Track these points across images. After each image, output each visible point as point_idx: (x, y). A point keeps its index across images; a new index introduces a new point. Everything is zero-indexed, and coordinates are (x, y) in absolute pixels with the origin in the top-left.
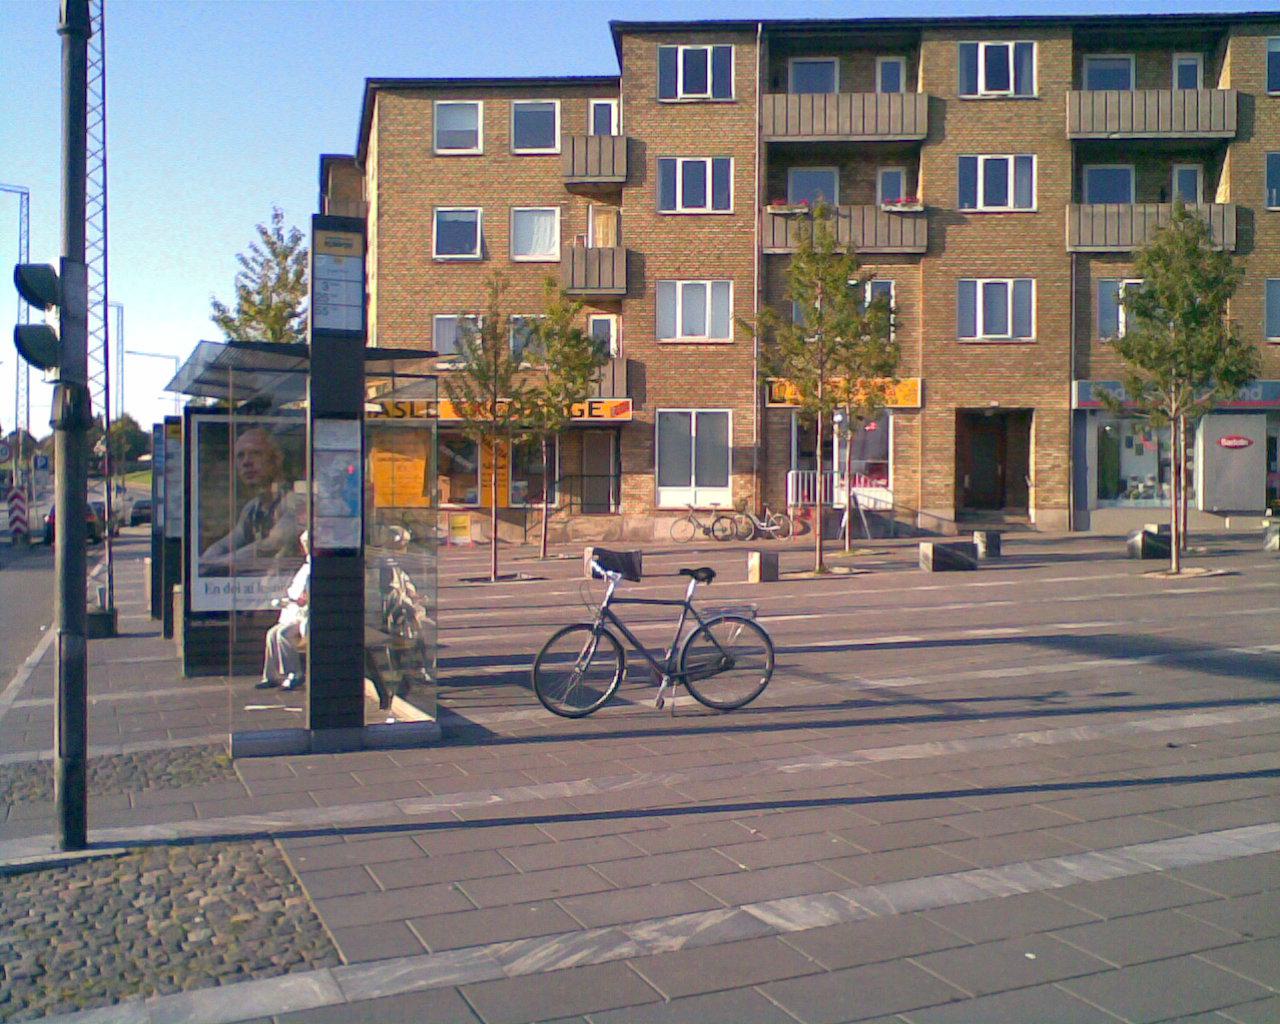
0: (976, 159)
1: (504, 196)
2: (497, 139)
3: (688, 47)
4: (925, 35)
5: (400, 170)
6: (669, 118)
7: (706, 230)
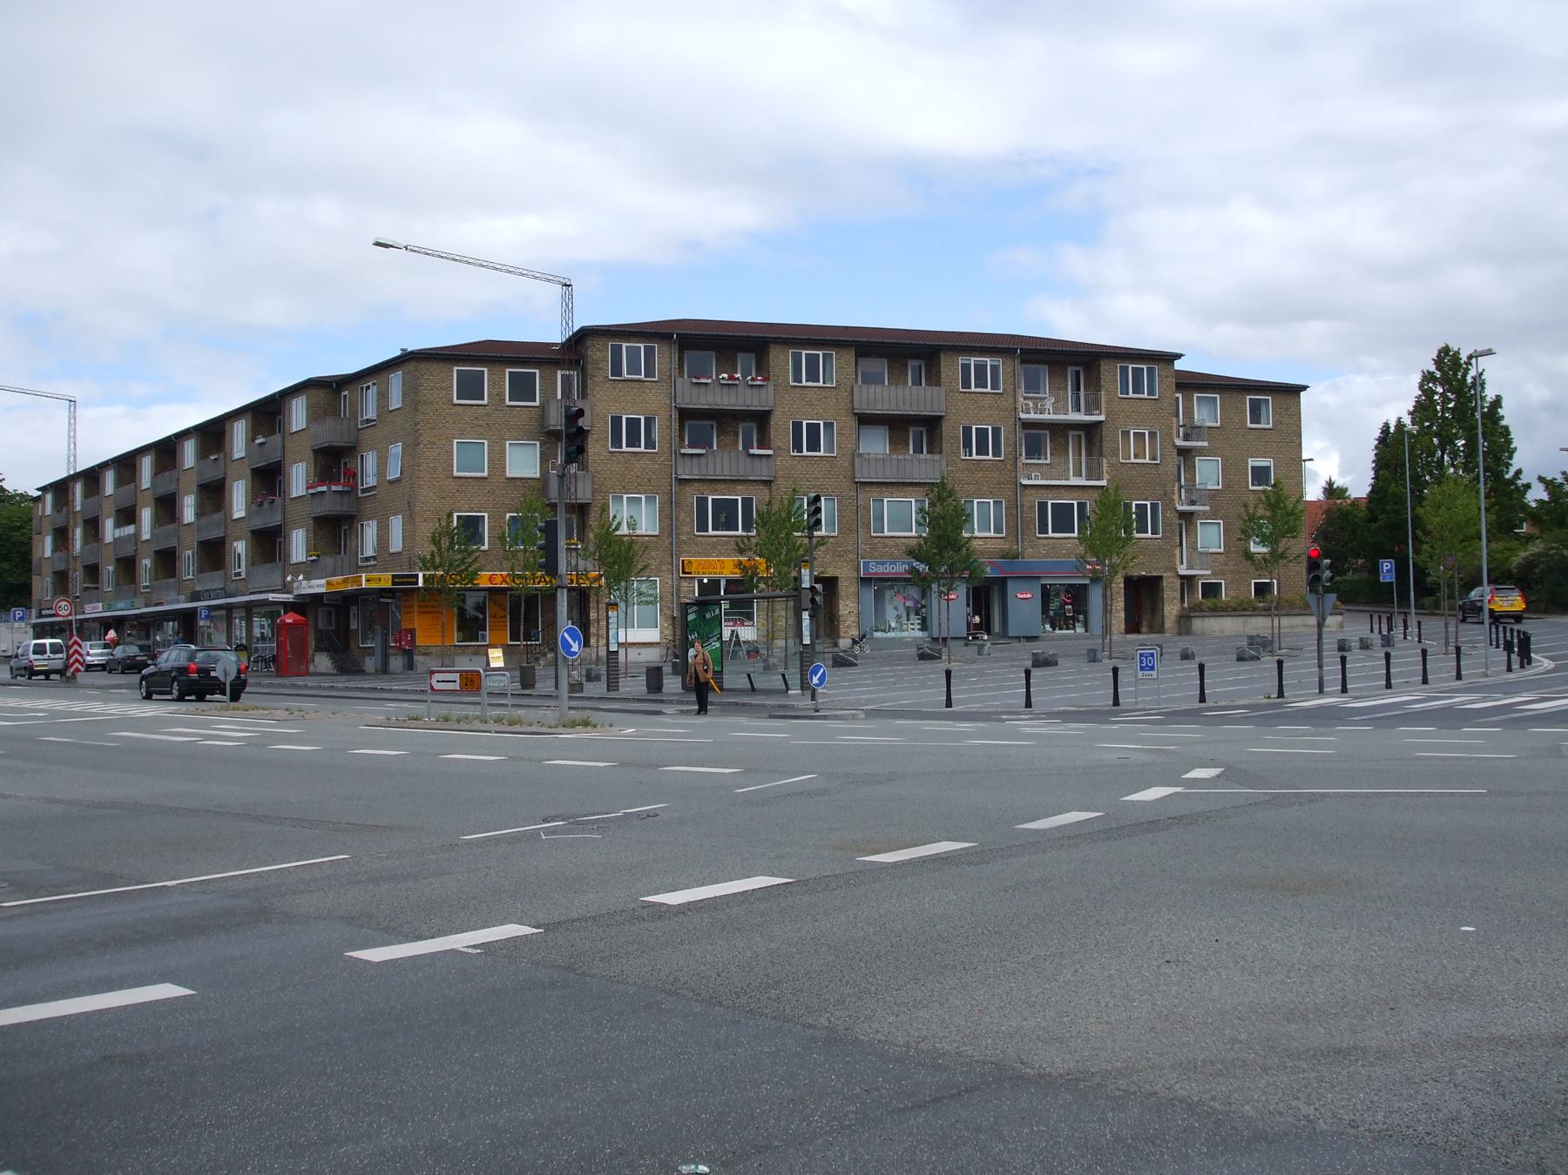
0: (971, 427)
1: (502, 433)
2: (498, 394)
3: (807, 352)
4: (771, 346)
5: (431, 414)
6: (617, 390)
7: (641, 462)
